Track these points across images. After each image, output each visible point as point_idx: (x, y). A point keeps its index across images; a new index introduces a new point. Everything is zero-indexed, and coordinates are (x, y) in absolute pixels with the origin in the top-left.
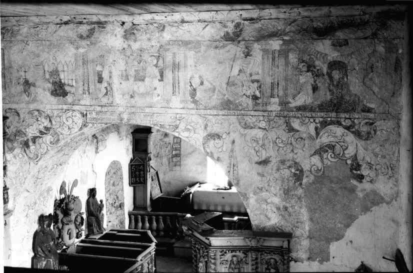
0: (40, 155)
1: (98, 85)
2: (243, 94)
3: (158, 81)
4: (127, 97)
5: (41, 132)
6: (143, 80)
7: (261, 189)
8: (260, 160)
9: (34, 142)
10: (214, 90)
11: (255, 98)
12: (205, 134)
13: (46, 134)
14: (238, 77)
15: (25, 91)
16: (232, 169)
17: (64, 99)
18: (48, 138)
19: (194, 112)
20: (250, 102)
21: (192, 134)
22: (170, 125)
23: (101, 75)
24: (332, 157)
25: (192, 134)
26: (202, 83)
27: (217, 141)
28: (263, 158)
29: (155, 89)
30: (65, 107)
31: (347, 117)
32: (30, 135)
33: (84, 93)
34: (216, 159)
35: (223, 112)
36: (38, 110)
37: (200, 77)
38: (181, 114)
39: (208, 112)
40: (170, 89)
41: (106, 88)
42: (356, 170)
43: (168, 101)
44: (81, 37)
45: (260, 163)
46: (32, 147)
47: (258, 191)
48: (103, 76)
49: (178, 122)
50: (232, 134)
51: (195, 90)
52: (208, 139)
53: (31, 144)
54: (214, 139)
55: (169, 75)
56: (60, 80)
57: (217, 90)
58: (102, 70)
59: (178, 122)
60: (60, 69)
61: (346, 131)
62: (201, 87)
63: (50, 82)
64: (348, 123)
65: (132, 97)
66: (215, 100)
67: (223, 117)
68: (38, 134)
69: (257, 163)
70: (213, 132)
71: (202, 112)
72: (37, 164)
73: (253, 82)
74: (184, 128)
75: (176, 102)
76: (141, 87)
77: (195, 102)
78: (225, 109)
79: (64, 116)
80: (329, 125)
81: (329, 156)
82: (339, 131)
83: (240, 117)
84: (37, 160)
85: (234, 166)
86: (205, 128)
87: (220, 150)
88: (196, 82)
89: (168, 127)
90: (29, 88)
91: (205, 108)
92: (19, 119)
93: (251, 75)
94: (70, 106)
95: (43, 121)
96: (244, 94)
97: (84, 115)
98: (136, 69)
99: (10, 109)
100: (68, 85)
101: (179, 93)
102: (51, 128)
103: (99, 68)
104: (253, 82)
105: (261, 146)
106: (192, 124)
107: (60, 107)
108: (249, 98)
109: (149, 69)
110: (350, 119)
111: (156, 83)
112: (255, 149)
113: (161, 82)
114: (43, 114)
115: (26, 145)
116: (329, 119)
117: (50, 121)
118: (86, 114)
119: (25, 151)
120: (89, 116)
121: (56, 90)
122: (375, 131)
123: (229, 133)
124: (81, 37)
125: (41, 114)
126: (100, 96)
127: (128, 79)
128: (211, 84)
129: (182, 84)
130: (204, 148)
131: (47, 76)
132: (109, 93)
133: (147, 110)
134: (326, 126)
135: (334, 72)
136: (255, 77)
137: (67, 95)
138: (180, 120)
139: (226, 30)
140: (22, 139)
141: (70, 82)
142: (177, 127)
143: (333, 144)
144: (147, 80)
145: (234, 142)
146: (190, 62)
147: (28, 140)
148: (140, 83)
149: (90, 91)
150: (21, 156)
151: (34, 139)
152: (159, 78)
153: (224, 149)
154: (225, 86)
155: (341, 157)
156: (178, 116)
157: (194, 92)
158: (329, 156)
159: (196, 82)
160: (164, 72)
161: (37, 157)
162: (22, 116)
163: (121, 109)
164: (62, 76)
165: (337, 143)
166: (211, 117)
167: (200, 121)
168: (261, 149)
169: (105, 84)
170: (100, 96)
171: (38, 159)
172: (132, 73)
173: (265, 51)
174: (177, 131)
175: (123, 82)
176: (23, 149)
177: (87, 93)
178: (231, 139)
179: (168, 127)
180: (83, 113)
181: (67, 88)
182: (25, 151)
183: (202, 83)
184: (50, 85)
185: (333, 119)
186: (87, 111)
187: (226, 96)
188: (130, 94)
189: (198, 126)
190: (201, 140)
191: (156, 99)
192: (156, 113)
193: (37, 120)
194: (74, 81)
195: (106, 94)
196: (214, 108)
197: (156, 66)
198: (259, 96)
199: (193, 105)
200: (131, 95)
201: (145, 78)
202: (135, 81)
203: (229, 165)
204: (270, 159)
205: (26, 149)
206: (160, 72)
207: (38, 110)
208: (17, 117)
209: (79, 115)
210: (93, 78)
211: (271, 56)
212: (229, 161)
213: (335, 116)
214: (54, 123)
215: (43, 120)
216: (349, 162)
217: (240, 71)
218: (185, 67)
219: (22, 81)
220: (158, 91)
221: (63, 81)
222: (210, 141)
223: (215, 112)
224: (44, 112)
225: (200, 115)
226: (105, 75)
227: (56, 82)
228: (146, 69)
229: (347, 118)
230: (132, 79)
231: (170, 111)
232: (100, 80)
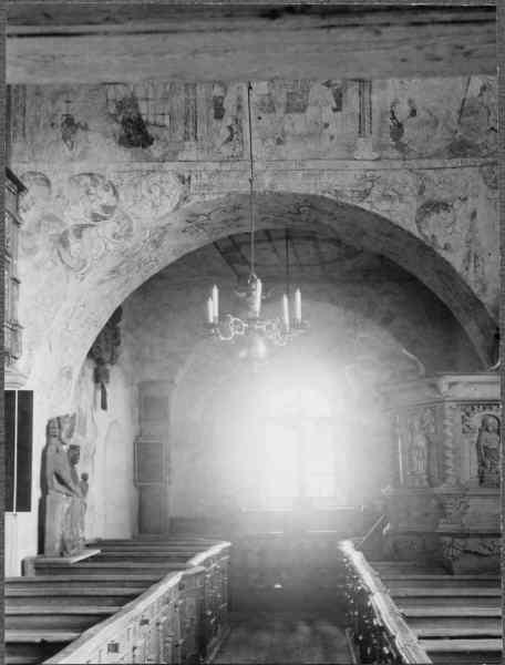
0: (89, 260)
3: (331, 111)
5: (95, 217)
9: (79, 236)
10: (437, 123)
12: (420, 204)
13: (105, 219)
14: (480, 100)
15: (65, 138)
16: (472, 264)
17: (146, 151)
18: (109, 227)
19: (398, 165)
21: (397, 203)
22: (354, 192)
23: (221, 105)
25: (397, 203)
27: (443, 214)
29: (327, 125)
30: (146, 166)
32: (71, 223)
34: (442, 246)
35: (455, 162)
36: (91, 175)
37: (410, 102)
38: (374, 170)
39: (425, 163)
40: (353, 127)
41: (230, 128)
46: (74, 245)
48: (225, 106)
49: (369, 185)
50: (470, 200)
51: (400, 126)
52: (427, 212)
53: (72, 239)
54: (438, 212)
55: (352, 98)
56: (139, 115)
57: (440, 125)
58: (222, 94)
59: (369, 185)
60: (140, 93)
62: (412, 119)
63: (117, 121)
65: (279, 142)
66: (440, 139)
68: (89, 221)
71: (414, 164)
72: (82, 279)
75: (365, 150)
76: (299, 123)
77: (401, 147)
78: (457, 156)
79: (144, 183)
83: (485, 168)
84: (83, 271)
85: (476, 257)
86: (421, 193)
87: (450, 230)
88: (403, 110)
89: (349, 194)
90: (74, 132)
91: (421, 157)
92: (50, 193)
94: (156, 164)
95: (100, 195)
97: (184, 180)
98: (290, 91)
99: (32, 173)
100: (155, 125)
102: (115, 207)
103: (217, 91)
106: (396, 187)
107: (137, 166)
114: (101, 181)
115: (63, 241)
117: (115, 193)
118: (189, 178)
120: (194, 181)
121: (129, 136)
125: (96, 181)
126: (219, 142)
127: (274, 110)
128: (431, 114)
129: (375, 116)
130: (420, 231)
131: (112, 110)
133: (310, 165)
137: (151, 143)
140: (54, 232)
141: (159, 119)
144: (309, 109)
145: (474, 215)
147: (66, 233)
148: (296, 116)
149: (199, 135)
150: (50, 264)
151: (80, 230)
152: (335, 105)
153: (457, 228)
154: (455, 115)
156: (368, 174)
159: (403, 110)
160: (344, 95)
161: (84, 266)
164: (143, 108)
166: (430, 173)
167: (410, 178)
169: (228, 121)
170: (219, 142)
171: (85, 269)
172: (282, 99)
174: (369, 199)
175: (261, 115)
176: (56, 252)
177: (192, 138)
178: (470, 211)
179: (349, 194)
180: (183, 177)
181: (151, 131)
183: (413, 113)
184: (117, 127)
186: (190, 171)
187: (459, 133)
188: (277, 137)
189: (407, 189)
190: (414, 213)
191: (326, 143)
192: (329, 170)
193: (88, 193)
194: (167, 117)
195: (230, 139)
196: (437, 155)
199: (396, 154)
201: (305, 107)
202: (287, 111)
205: (62, 250)
206: (335, 96)
207: (91, 175)
208: (46, 190)
209: (173, 180)
210: (205, 110)
212: (466, 249)
214: (122, 197)
215: (101, 193)
219: (59, 120)
220: (332, 130)
221: (144, 118)
222: (430, 216)
223: (437, 163)
224: (102, 177)
225: (411, 170)
226: (229, 105)
227: (130, 120)
228: (308, 91)
230: (280, 112)
231: (352, 164)
232: (219, 114)
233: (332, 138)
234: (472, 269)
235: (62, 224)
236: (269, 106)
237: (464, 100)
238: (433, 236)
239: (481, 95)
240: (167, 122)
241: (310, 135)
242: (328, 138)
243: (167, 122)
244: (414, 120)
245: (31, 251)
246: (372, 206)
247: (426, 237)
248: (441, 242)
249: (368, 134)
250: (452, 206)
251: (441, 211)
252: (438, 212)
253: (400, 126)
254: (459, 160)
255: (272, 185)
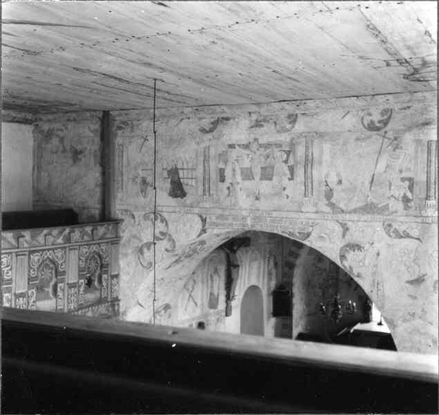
1: (220, 184)
2: (390, 195)
4: (252, 198)
6: (271, 179)
7: (413, 315)
8: (412, 279)
11: (406, 200)
13: (161, 239)
20: (400, 206)
26: (340, 182)
28: (415, 277)
29: (284, 189)
33: (204, 194)
34: (356, 274)
37: (338, 175)
41: (228, 188)
43: (301, 204)
44: (204, 131)
45: (411, 282)
47: (408, 317)
50: (376, 244)
53: (145, 250)
54: (354, 250)
55: (300, 172)
57: (358, 190)
58: (224, 167)
65: (257, 199)
67: (366, 224)
69: (409, 282)
70: (352, 242)
73: (403, 180)
74: (316, 236)
76: (265, 187)
85: (378, 284)
87: (361, 264)
88: (333, 179)
92: (135, 222)
93: (401, 171)
96: (392, 196)
98: (263, 166)
101: (312, 194)
103: (221, 165)
104: (403, 180)
105: (414, 261)
108: (398, 200)
109: (277, 165)
111: (286, 182)
112: (405, 265)
113: (291, 181)
115: (141, 251)
118: (206, 219)
119: (139, 258)
123: (372, 243)
124: (204, 131)
132: (231, 194)
133: (275, 214)
136: (404, 175)
138: (312, 226)
139: (371, 118)
142: (308, 235)
144: (275, 178)
146: (326, 157)
152: (289, 176)
156: (310, 222)
157: (329, 194)
159: (333, 179)
162: (137, 220)
163: (244, 213)
168: (413, 264)
169: (227, 184)
173: (418, 142)
177: (207, 194)
178: (375, 251)
179: (298, 235)
182: (139, 258)
183: (340, 182)
192: (286, 218)
195: (229, 195)
196: (355, 211)
197: (286, 162)
198: (411, 198)
200: (256, 197)
201: (272, 176)
202: (261, 179)
203: (372, 283)
204: (425, 277)
205: (141, 256)
206: (289, 170)
210: (214, 176)
211: (425, 148)
217: (388, 166)
218: (320, 163)
219: (139, 180)
220: (286, 192)
226: (228, 173)
230: (257, 178)
231: (302, 216)
232: (223, 180)
233: (288, 197)
234: (375, 292)
235: (141, 241)
236: (248, 175)
237: (374, 175)
238: (350, 267)
239: (385, 172)
240: (194, 184)
241: (276, 194)
242: (285, 197)
243: (194, 184)
244: (340, 187)
245: (126, 255)
246: (312, 243)
247: (345, 267)
248: (355, 271)
249: (310, 195)
250: (363, 248)
251: (356, 250)
252: (354, 250)
253: (331, 190)
254: (369, 216)
255: (252, 226)
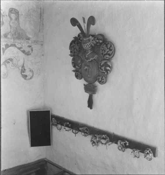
24: (12, 66)
31: (19, 42)
42: (24, 72)
61: (19, 50)
64: (19, 46)
80: (10, 47)
81: (10, 65)
82: (15, 50)
110: (20, 43)
116: (10, 43)
122: (32, 50)
134: (8, 47)
135: (12, 15)
143: (12, 58)
155: (16, 65)
158: (10, 65)
165: (15, 57)
185: (12, 43)
213: (13, 42)
216: (20, 68)
229: (19, 43)
